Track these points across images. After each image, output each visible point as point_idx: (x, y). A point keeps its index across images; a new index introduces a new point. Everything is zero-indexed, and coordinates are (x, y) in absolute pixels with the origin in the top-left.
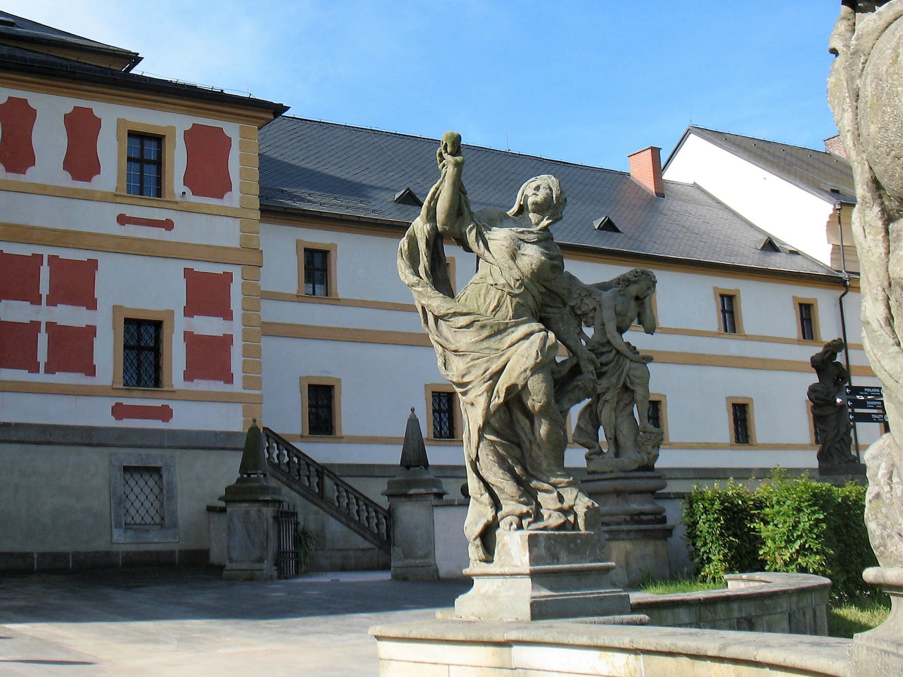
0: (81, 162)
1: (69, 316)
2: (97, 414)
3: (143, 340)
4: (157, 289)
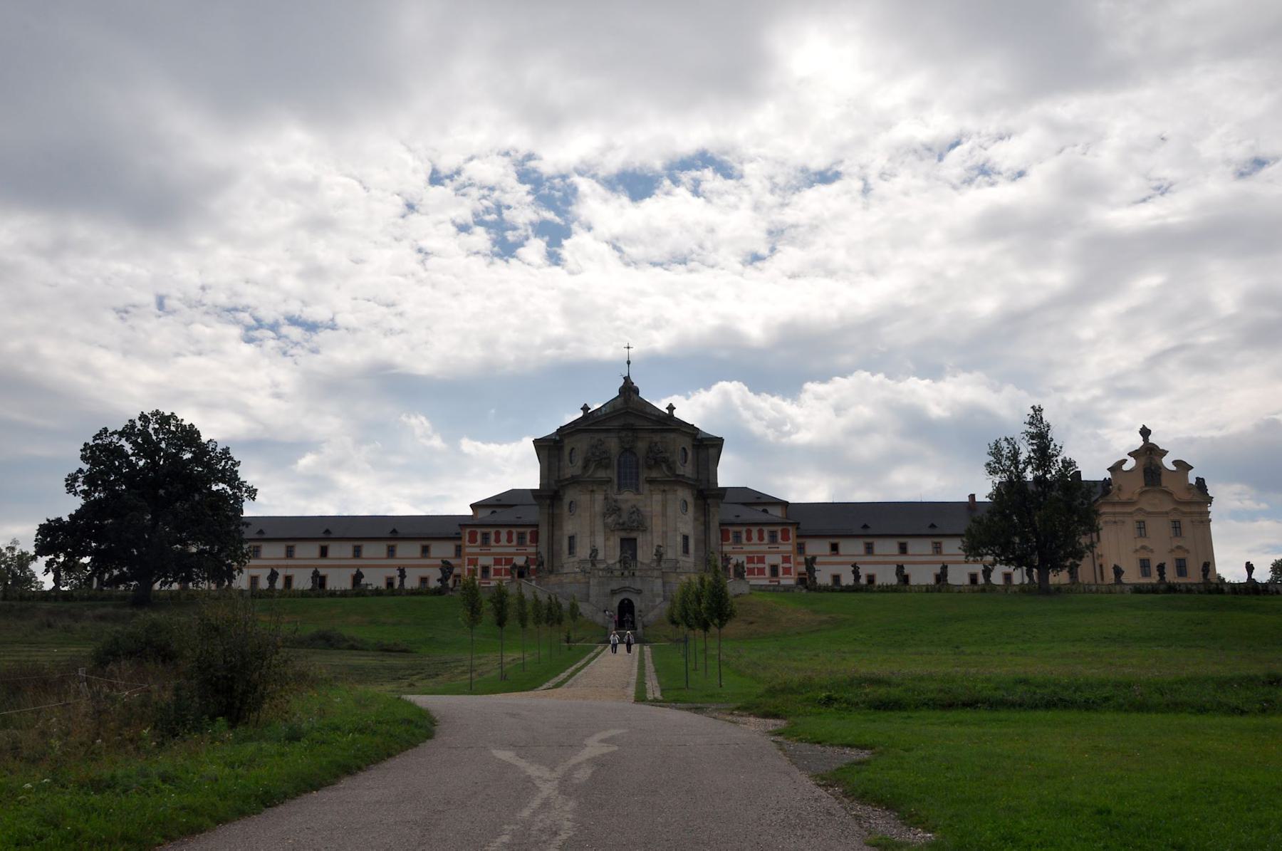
0: (761, 538)
1: (760, 566)
2: (766, 582)
3: (774, 569)
4: (777, 559)
